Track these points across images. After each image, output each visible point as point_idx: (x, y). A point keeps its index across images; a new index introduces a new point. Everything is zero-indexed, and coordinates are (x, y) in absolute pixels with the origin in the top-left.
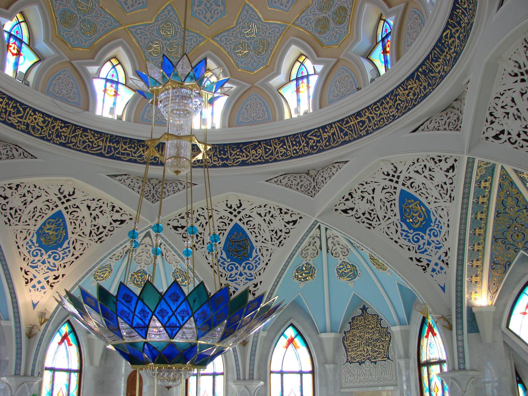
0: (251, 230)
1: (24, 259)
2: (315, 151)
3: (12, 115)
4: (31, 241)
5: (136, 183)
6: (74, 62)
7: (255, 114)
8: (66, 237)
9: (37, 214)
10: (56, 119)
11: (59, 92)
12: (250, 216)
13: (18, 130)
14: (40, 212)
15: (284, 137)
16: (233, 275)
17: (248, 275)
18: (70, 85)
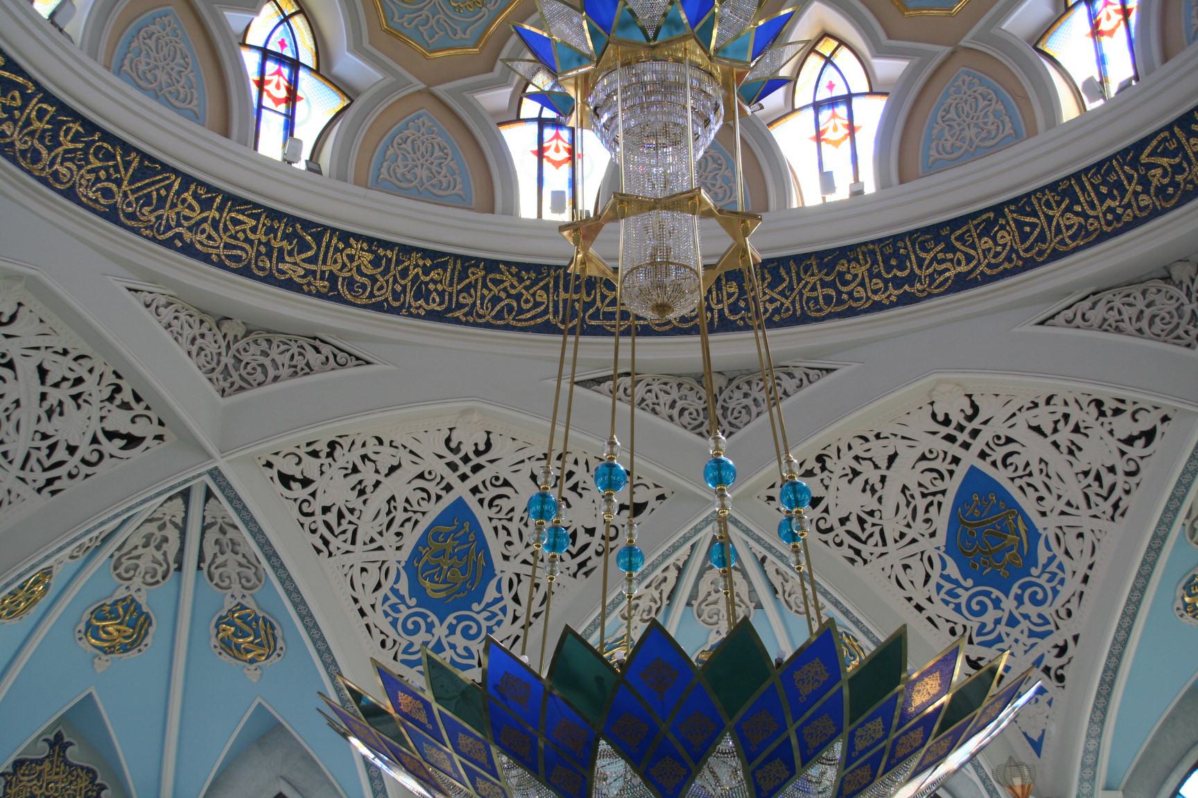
0: (1022, 482)
1: (383, 644)
2: (1173, 201)
3: (287, 258)
4: (395, 591)
5: (661, 394)
6: (439, 90)
7: (973, 131)
8: (489, 572)
9: (400, 516)
10: (406, 250)
11: (409, 176)
12: (1009, 440)
13: (309, 293)
14: (405, 510)
15: (1068, 178)
16: (990, 627)
17: (1035, 619)
18: (437, 153)
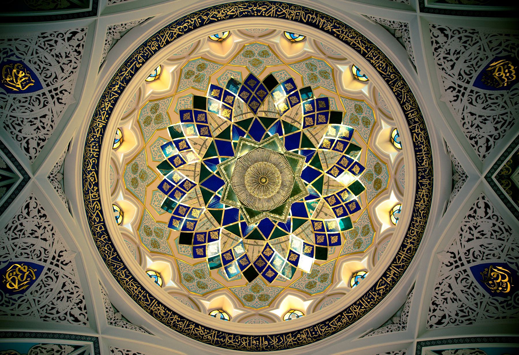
10: (174, 313)
15: (358, 300)
